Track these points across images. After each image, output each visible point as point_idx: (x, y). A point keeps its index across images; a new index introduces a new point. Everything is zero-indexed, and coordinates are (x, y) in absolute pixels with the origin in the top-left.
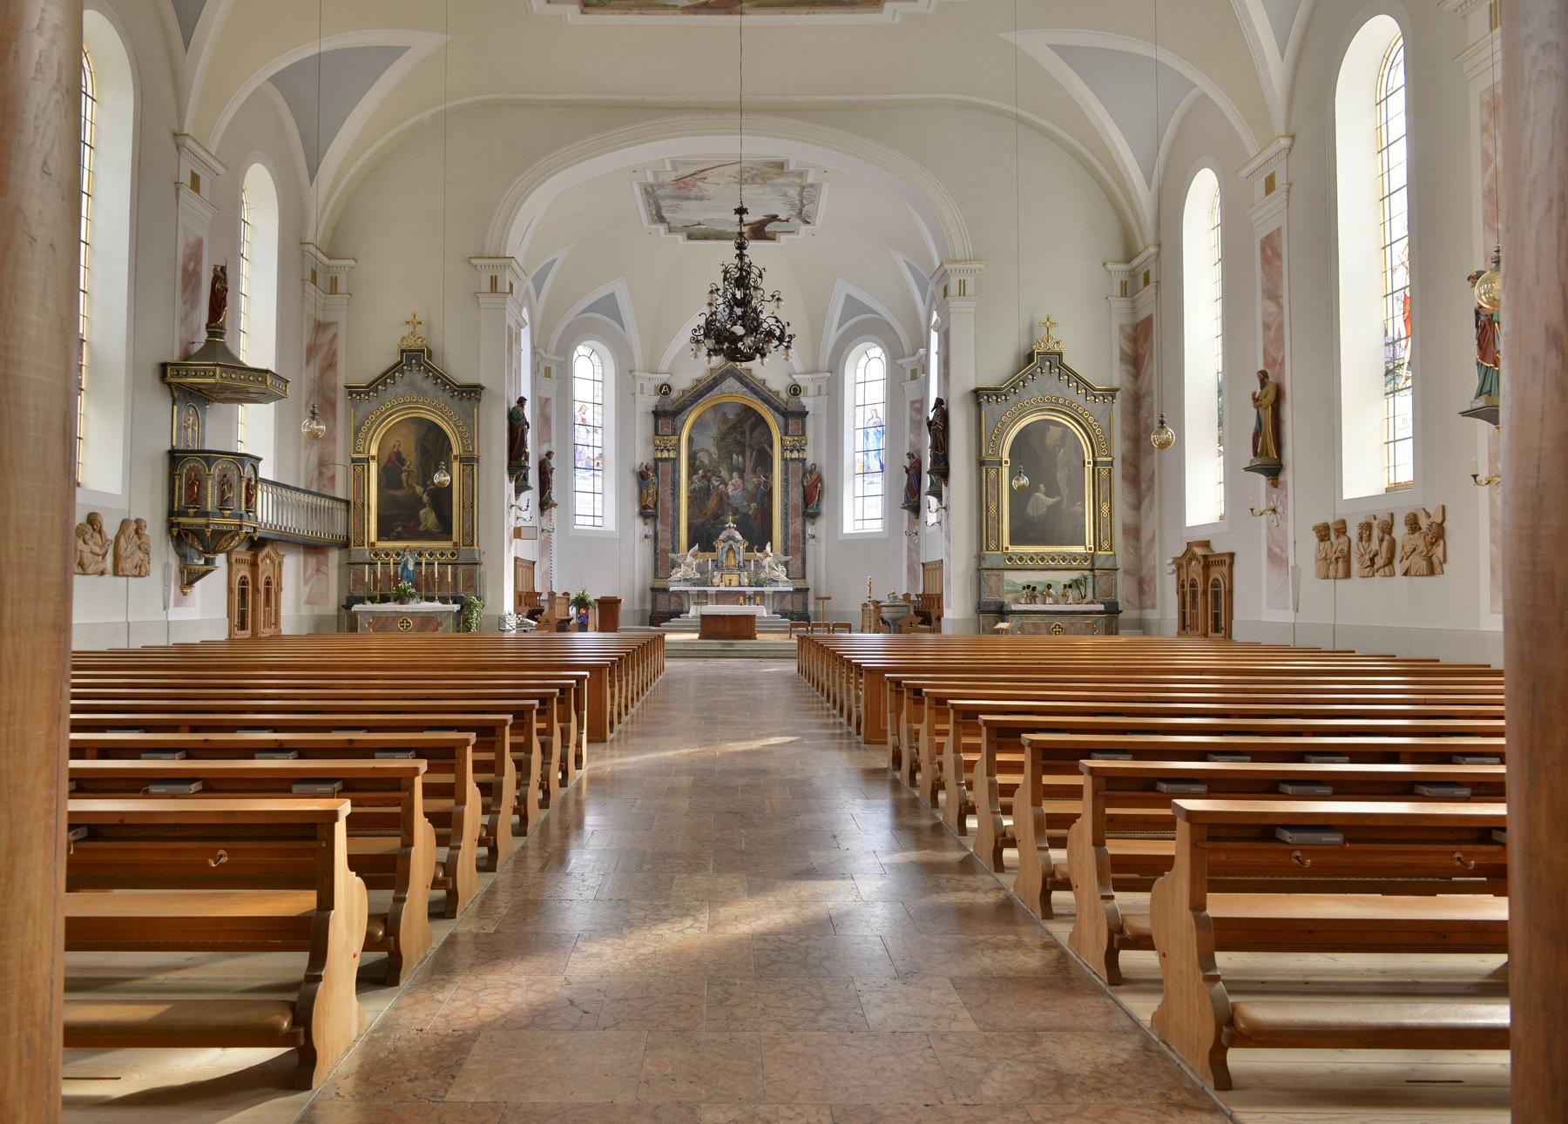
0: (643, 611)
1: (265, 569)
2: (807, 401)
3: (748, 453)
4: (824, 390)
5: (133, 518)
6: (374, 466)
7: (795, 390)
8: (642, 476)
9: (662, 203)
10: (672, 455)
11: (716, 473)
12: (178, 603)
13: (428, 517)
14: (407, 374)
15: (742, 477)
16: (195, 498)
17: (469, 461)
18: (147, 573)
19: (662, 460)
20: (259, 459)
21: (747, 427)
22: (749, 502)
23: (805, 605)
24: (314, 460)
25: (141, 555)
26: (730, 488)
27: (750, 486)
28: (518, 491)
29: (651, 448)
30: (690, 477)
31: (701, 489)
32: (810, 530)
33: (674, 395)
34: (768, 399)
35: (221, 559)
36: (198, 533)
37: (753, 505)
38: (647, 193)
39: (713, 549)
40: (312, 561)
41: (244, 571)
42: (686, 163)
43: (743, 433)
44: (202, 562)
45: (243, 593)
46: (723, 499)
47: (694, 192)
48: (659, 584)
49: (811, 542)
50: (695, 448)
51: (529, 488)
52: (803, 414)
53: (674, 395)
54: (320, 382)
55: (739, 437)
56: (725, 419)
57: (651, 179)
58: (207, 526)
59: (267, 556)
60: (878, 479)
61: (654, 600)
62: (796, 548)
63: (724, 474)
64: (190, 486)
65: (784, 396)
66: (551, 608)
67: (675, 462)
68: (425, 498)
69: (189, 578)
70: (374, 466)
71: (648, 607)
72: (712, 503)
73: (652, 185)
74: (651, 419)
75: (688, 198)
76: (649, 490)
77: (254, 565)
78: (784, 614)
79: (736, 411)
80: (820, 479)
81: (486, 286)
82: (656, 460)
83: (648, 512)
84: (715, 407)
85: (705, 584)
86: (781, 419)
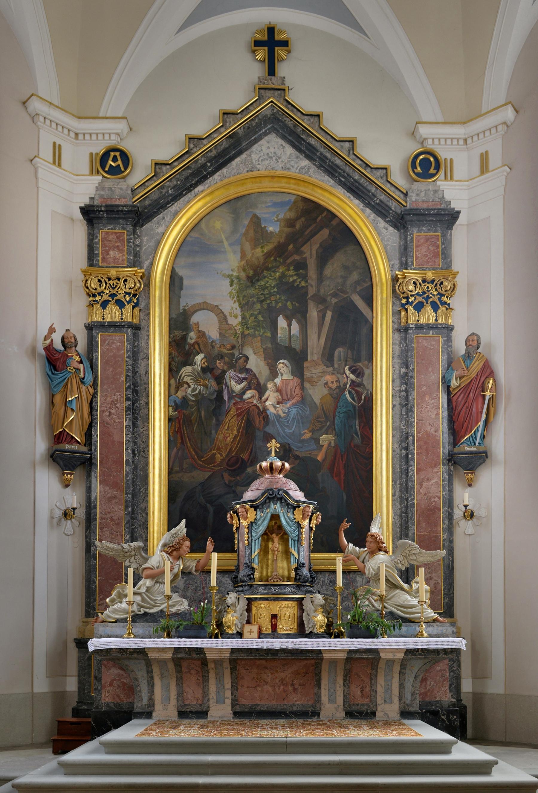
0: (59, 697)
2: (453, 191)
3: (313, 313)
4: (495, 160)
7: (427, 165)
10: (128, 314)
15: (298, 370)
21: (310, 252)
22: (317, 431)
26: (271, 399)
27: (317, 394)
29: (83, 300)
30: (173, 370)
31: (200, 399)
32: (464, 496)
33: (138, 174)
37: (326, 439)
39: (226, 543)
43: (300, 266)
46: (254, 426)
52: (448, 218)
53: (138, 174)
55: (292, 276)
63: (256, 363)
67: (138, 330)
71: (72, 685)
72: (228, 432)
74: (81, 230)
79: (284, 214)
82: (90, 328)
84: (235, 205)
85: (198, 631)
86: (392, 234)
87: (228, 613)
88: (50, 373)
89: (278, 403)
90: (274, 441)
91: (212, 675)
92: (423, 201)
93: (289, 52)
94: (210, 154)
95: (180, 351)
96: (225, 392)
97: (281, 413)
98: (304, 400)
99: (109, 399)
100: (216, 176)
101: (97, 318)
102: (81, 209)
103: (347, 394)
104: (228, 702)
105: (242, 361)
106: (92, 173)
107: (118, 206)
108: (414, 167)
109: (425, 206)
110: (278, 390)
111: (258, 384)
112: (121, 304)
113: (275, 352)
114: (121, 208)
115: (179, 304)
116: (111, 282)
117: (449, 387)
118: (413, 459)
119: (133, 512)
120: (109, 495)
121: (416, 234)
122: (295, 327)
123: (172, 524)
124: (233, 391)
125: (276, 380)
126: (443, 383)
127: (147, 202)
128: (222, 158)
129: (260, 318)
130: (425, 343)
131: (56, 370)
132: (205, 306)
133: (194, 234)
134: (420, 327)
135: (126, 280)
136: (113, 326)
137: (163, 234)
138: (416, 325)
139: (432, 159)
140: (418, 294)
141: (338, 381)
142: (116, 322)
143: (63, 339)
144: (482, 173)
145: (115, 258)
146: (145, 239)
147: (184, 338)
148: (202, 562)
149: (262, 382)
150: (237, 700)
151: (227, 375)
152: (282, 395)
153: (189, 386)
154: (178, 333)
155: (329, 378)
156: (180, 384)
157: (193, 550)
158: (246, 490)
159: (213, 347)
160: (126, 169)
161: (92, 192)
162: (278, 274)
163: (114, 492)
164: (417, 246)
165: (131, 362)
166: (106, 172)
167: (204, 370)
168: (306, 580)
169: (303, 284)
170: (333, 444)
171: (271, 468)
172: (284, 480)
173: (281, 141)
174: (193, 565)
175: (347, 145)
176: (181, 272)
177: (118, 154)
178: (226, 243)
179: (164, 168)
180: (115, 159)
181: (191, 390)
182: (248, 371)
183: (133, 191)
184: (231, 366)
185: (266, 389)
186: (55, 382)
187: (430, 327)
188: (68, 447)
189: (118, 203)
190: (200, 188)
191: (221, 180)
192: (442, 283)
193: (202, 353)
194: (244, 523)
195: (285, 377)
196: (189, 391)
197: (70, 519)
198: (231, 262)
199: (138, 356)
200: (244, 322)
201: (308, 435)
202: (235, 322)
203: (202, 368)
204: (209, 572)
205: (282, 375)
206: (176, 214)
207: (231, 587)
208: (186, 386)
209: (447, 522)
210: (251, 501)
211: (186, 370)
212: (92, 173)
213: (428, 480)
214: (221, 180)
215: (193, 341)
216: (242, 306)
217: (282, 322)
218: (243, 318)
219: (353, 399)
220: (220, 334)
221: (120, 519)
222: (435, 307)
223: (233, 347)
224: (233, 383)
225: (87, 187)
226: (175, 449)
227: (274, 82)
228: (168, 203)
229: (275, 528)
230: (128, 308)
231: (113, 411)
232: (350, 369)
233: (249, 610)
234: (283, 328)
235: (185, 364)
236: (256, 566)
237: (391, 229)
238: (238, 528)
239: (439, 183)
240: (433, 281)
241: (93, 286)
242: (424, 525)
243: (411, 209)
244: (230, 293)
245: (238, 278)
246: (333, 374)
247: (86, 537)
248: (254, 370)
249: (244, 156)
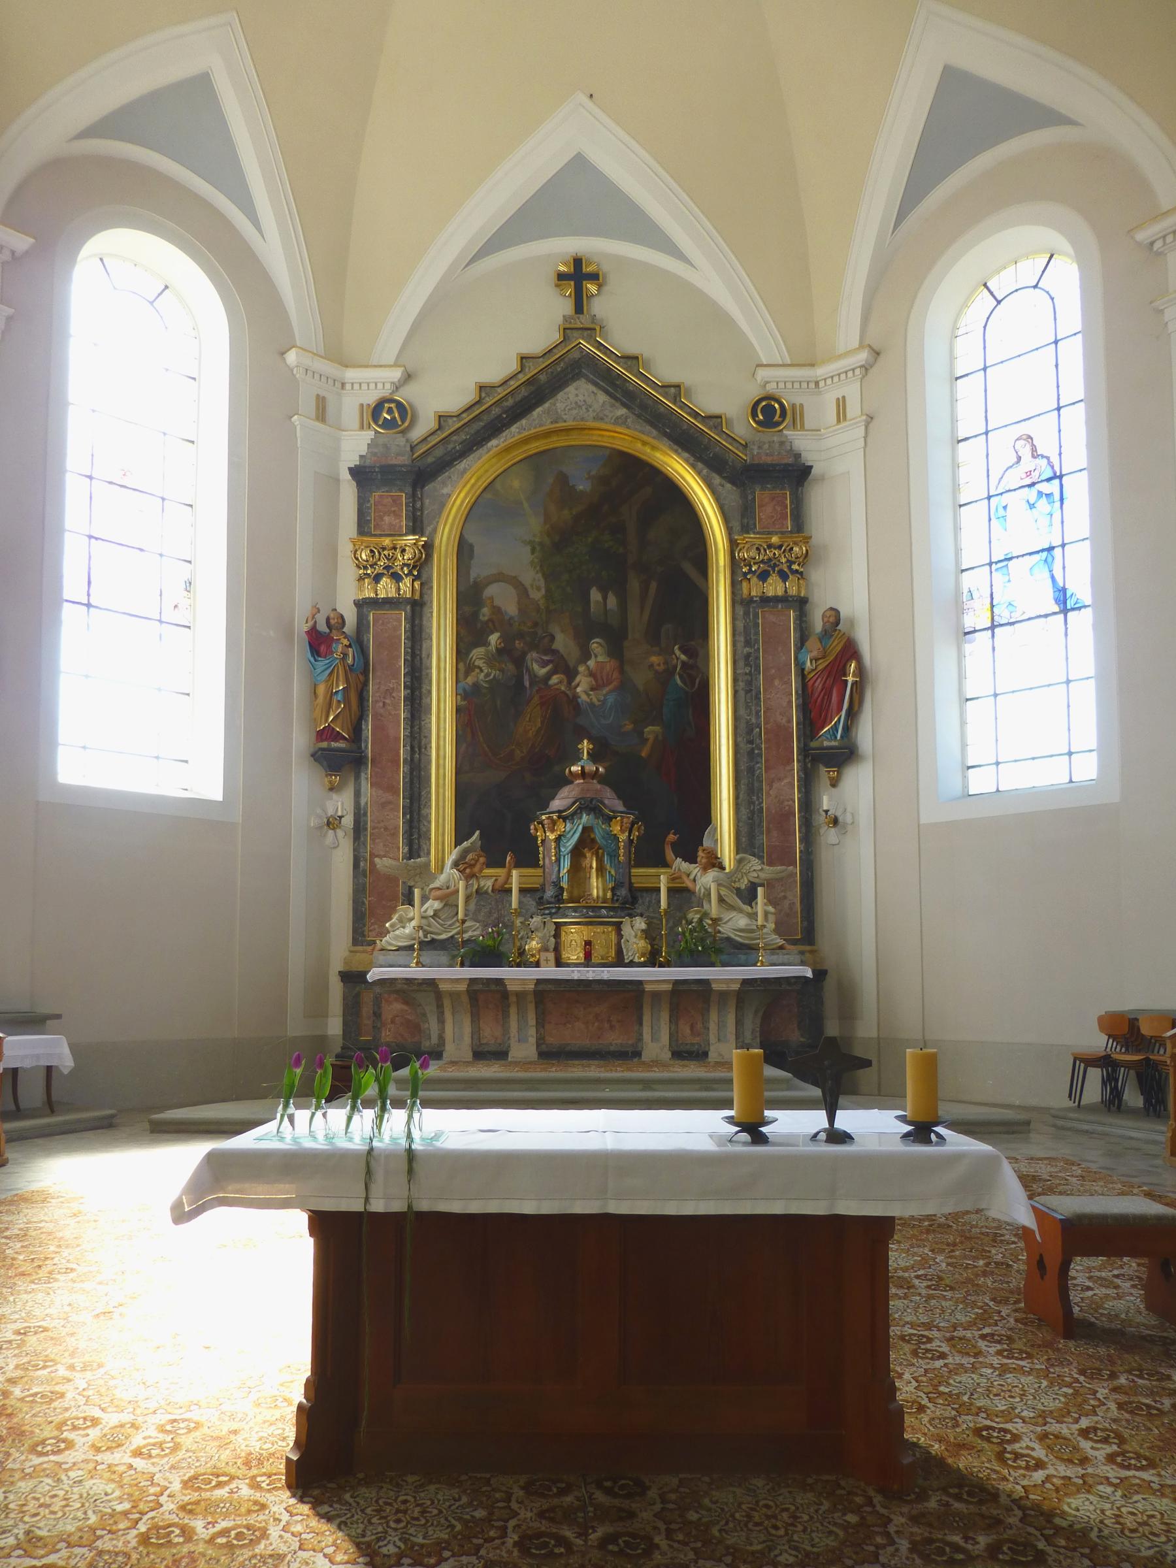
8: (318, 642)
15: (616, 649)
19: (374, 603)
26: (582, 685)
27: (641, 678)
30: (461, 653)
31: (494, 684)
37: (651, 731)
39: (528, 856)
46: (564, 719)
49: (829, 836)
50: (477, 571)
56: (564, 490)
62: (790, 841)
63: (563, 642)
65: (743, 427)
67: (417, 607)
71: (335, 1027)
72: (530, 724)
74: (348, 493)
76: (336, 692)
80: (850, 651)
82: (360, 604)
87: (533, 939)
88: (312, 660)
89: (592, 689)
90: (585, 742)
91: (513, 1011)
92: (767, 455)
93: (600, 286)
94: (505, 404)
95: (470, 631)
96: (526, 677)
97: (595, 700)
98: (625, 685)
99: (383, 688)
100: (514, 429)
101: (368, 593)
102: (350, 469)
103: (677, 677)
104: (533, 1040)
105: (546, 640)
106: (362, 428)
107: (396, 465)
108: (754, 414)
109: (769, 460)
110: (591, 674)
111: (567, 666)
112: (396, 577)
113: (586, 630)
114: (398, 469)
115: (469, 573)
116: (386, 552)
117: (803, 670)
118: (760, 755)
119: (411, 821)
120: (383, 800)
121: (761, 495)
122: (612, 601)
123: (460, 836)
124: (535, 676)
125: (589, 663)
126: (796, 665)
127: (430, 460)
129: (569, 590)
130: (772, 618)
131: (319, 656)
132: (500, 578)
133: (488, 496)
134: (765, 600)
135: (403, 551)
136: (388, 603)
137: (449, 496)
138: (761, 597)
139: (777, 406)
140: (762, 561)
141: (666, 663)
142: (392, 598)
143: (328, 619)
144: (839, 421)
145: (390, 524)
146: (427, 502)
147: (475, 614)
148: (501, 880)
149: (571, 664)
150: (543, 1039)
151: (529, 657)
152: (596, 681)
153: (482, 671)
154: (467, 609)
155: (654, 659)
156: (470, 668)
157: (489, 865)
158: (553, 798)
159: (511, 625)
160: (403, 422)
161: (364, 450)
162: (590, 540)
163: (388, 796)
164: (760, 506)
165: (409, 645)
166: (379, 426)
167: (500, 651)
168: (629, 899)
169: (621, 550)
170: (660, 738)
171: (583, 774)
172: (599, 786)
173: (592, 388)
174: (488, 884)
175: (673, 390)
176: (470, 538)
177: (393, 405)
178: (526, 505)
179: (450, 421)
180: (390, 411)
181: (483, 674)
182: (555, 652)
183: (412, 448)
184: (534, 646)
185: (577, 673)
186: (319, 671)
187: (776, 599)
188: (334, 745)
189: (394, 462)
190: (494, 442)
191: (519, 433)
192: (792, 549)
193: (497, 631)
194: (552, 836)
195: (600, 659)
196: (482, 676)
197: (334, 829)
198: (533, 525)
199: (417, 635)
200: (549, 596)
201: (629, 727)
202: (537, 595)
203: (497, 649)
204: (510, 891)
205: (596, 656)
206: (465, 471)
207: (533, 909)
208: (477, 670)
209: (803, 830)
210: (559, 812)
211: (477, 653)
212: (362, 428)
213: (780, 779)
214: (519, 433)
215: (486, 618)
216: (545, 576)
217: (595, 595)
218: (548, 590)
219: (685, 684)
220: (520, 610)
221: (397, 828)
222: (784, 577)
223: (536, 624)
224: (535, 666)
225: (356, 444)
226: (464, 746)
227: (584, 321)
228: (456, 459)
230: (407, 581)
231: (388, 701)
232: (680, 649)
233: (557, 936)
234: (597, 602)
235: (476, 645)
236: (564, 884)
237: (729, 486)
238: (543, 841)
239: (785, 432)
240: (780, 547)
241: (364, 557)
242: (775, 833)
243: (753, 465)
244: (532, 562)
245: (541, 544)
246: (659, 655)
247: (354, 850)
248: (562, 650)
249: (547, 405)
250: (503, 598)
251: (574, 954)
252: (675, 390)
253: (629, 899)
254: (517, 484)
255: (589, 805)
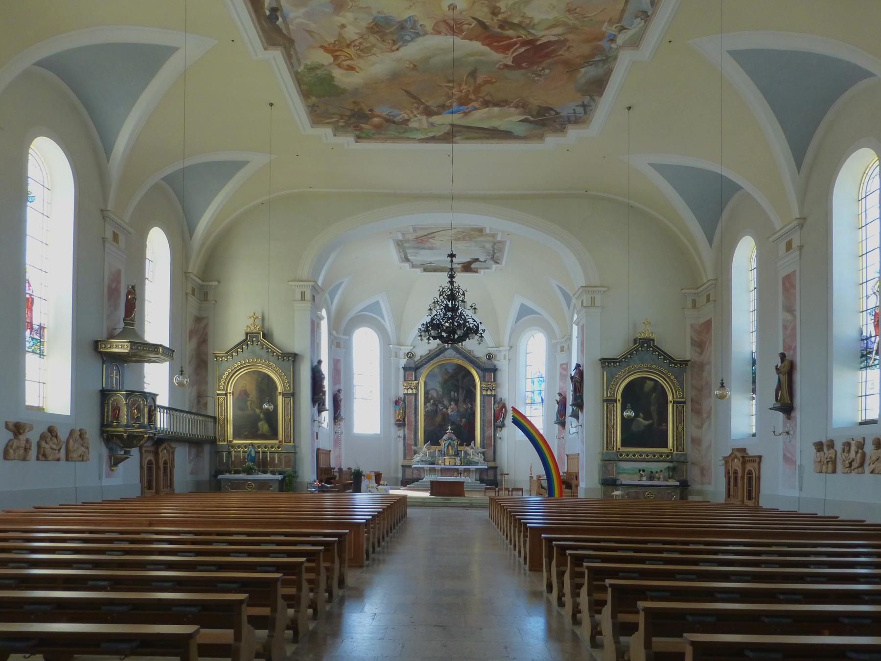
1: (163, 455)
3: (460, 391)
5: (78, 429)
6: (230, 398)
9: (408, 251)
10: (414, 391)
11: (441, 402)
12: (108, 476)
13: (263, 427)
14: (250, 346)
15: (457, 404)
16: (117, 417)
17: (292, 395)
18: (87, 459)
20: (157, 395)
23: (495, 476)
24: (194, 394)
25: (83, 449)
26: (449, 411)
27: (462, 410)
28: (320, 411)
30: (425, 404)
33: (417, 358)
34: (474, 362)
35: (135, 452)
36: (120, 437)
38: (398, 245)
39: (439, 445)
40: (193, 451)
41: (150, 457)
42: (422, 229)
43: (457, 380)
44: (122, 452)
45: (150, 469)
46: (445, 417)
47: (428, 245)
48: (407, 463)
49: (499, 441)
50: (428, 388)
51: (326, 410)
54: (196, 349)
57: (400, 237)
58: (125, 432)
59: (165, 448)
60: (540, 407)
61: (404, 472)
62: (491, 445)
64: (114, 410)
66: (340, 477)
67: (416, 395)
68: (262, 416)
69: (115, 461)
70: (230, 398)
72: (439, 419)
73: (401, 241)
75: (423, 248)
76: (401, 411)
77: (156, 454)
78: (482, 481)
81: (298, 297)
83: (401, 423)
95: (427, 400)
113: (451, 400)
128: (438, 355)
168: (457, 454)
181: (429, 408)
198: (440, 379)
229: (450, 444)
250: (434, 394)
251: (447, 463)
252: (470, 352)
253: (457, 454)
254: (437, 370)
255: (450, 438)
